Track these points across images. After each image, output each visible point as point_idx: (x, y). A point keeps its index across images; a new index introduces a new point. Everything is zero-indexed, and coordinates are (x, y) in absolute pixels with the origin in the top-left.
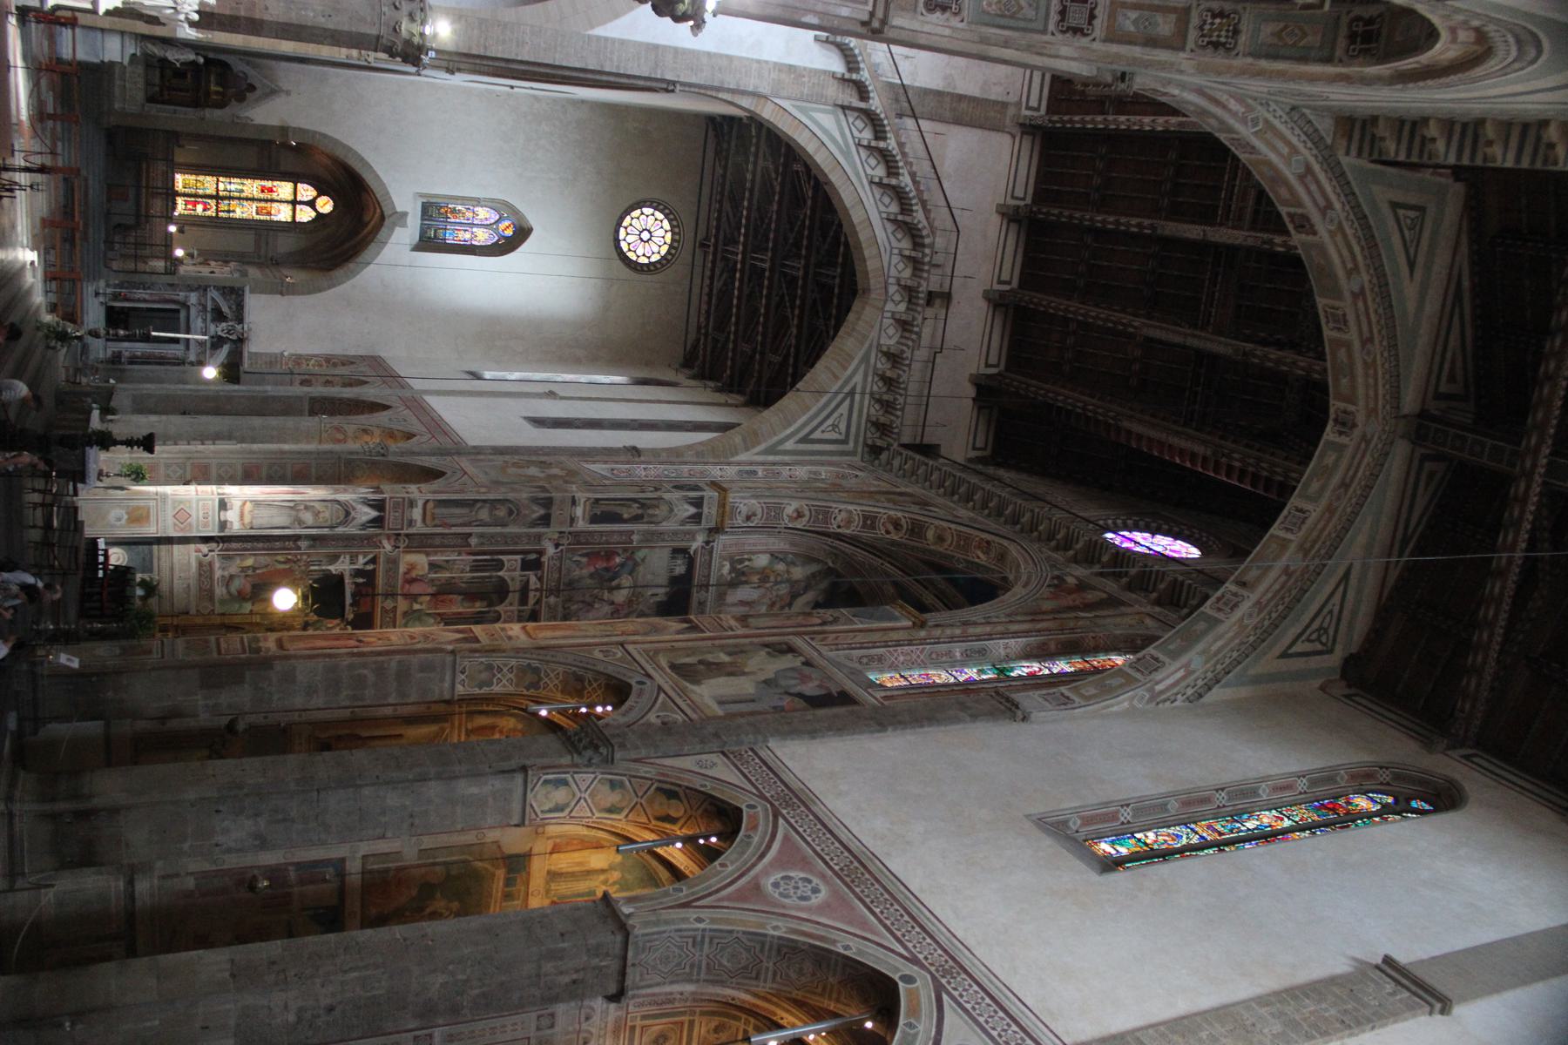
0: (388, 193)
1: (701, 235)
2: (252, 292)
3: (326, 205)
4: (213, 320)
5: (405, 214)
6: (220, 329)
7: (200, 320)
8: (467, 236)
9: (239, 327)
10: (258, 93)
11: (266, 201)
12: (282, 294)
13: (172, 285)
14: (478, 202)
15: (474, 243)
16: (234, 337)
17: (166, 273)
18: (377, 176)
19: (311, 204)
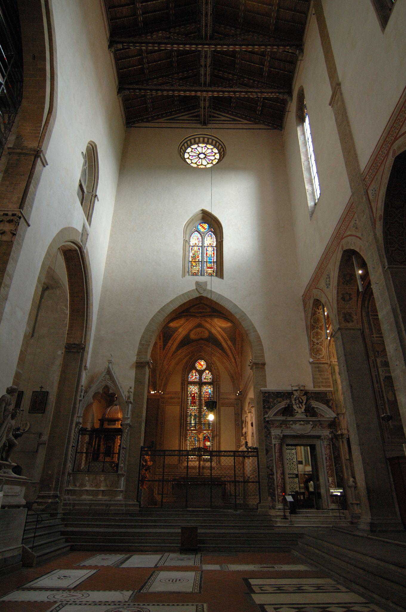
0: (183, 295)
1: (199, 126)
2: (266, 386)
3: (201, 364)
4: (292, 415)
5: (197, 283)
6: (300, 411)
7: (293, 426)
8: (210, 249)
9: (296, 394)
10: (110, 384)
11: (200, 400)
12: (264, 364)
13: (267, 451)
14: (186, 242)
15: (215, 244)
16: (304, 398)
17: (257, 456)
18: (171, 302)
19: (201, 372)
